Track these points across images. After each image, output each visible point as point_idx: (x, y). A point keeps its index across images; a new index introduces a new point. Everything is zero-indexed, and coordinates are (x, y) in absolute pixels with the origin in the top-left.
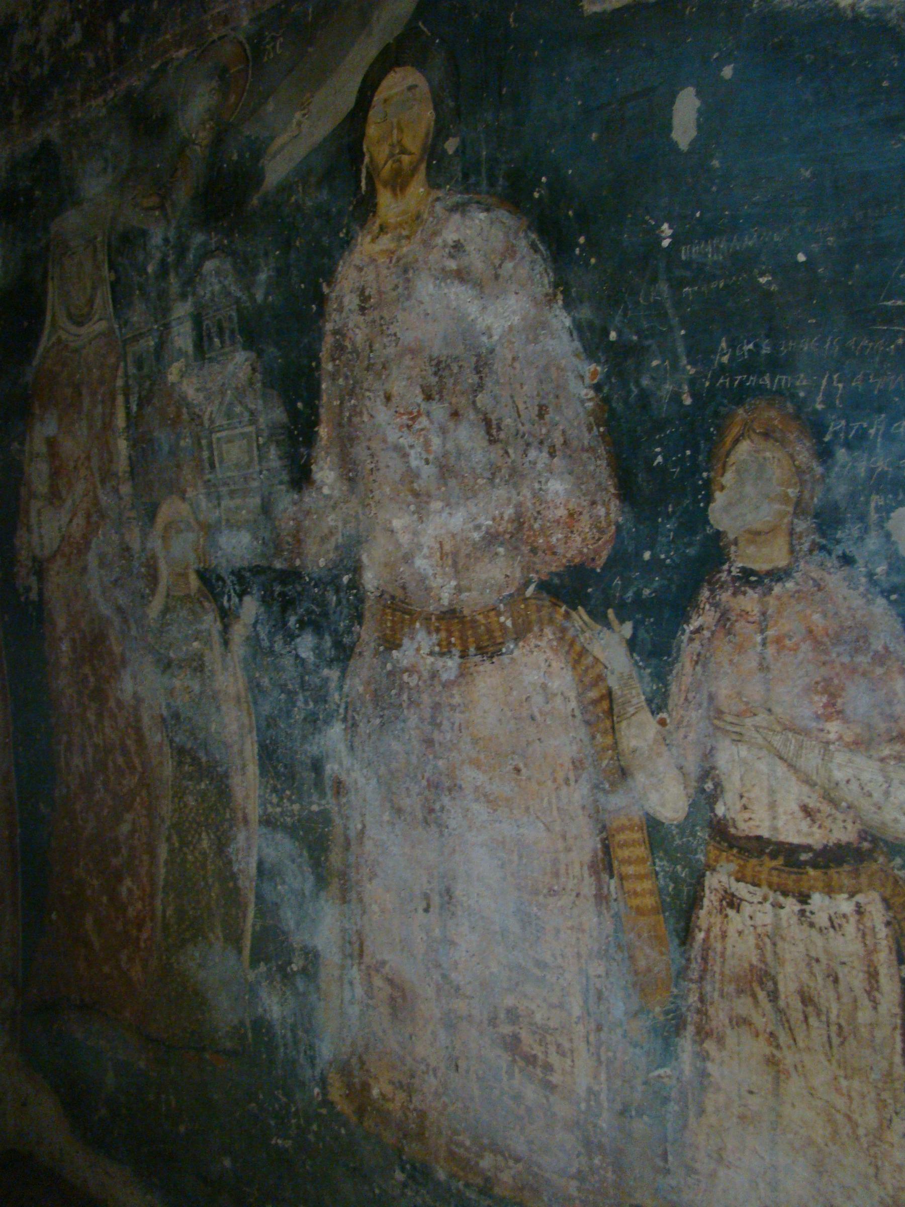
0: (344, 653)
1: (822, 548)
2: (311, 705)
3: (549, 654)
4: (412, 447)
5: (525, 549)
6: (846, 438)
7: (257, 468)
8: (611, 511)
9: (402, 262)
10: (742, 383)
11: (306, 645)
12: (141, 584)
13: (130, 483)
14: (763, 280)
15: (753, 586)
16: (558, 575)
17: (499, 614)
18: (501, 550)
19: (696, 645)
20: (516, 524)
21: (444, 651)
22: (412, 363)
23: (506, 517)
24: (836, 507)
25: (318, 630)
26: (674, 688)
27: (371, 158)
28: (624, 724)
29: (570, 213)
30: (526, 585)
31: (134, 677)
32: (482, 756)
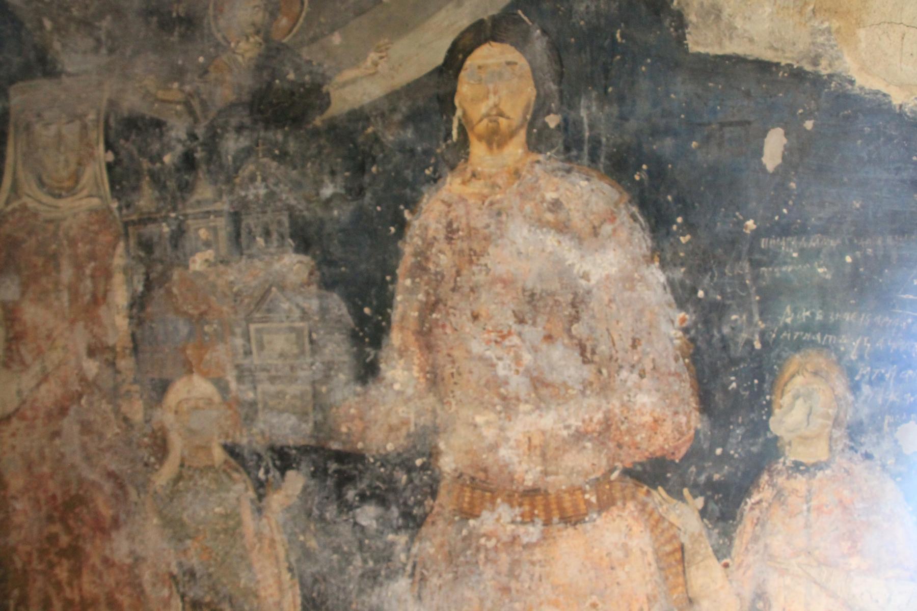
0: (413, 522)
1: (852, 448)
2: (371, 564)
3: (630, 521)
4: (500, 359)
5: (612, 445)
6: (870, 378)
7: (309, 360)
8: (693, 420)
9: (496, 206)
10: (799, 337)
11: (368, 515)
12: (144, 453)
13: (133, 358)
14: (820, 270)
15: (802, 473)
16: (641, 464)
17: (584, 492)
18: (589, 445)
19: (757, 512)
20: (604, 426)
21: (528, 519)
22: (503, 291)
23: (595, 420)
24: (861, 423)
25: (383, 501)
26: (737, 542)
27: (465, 113)
28: (693, 569)
29: (669, 198)
30: (612, 471)
31: (131, 537)
32: (561, 598)
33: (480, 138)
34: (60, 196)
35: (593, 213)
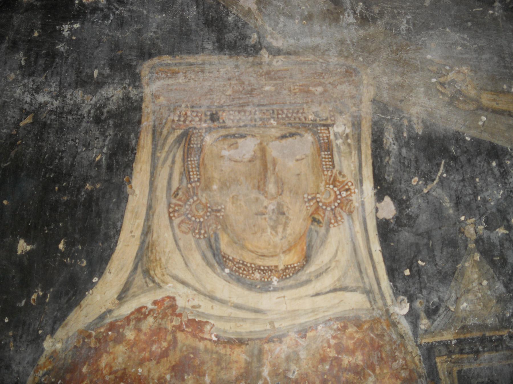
34: (265, 287)
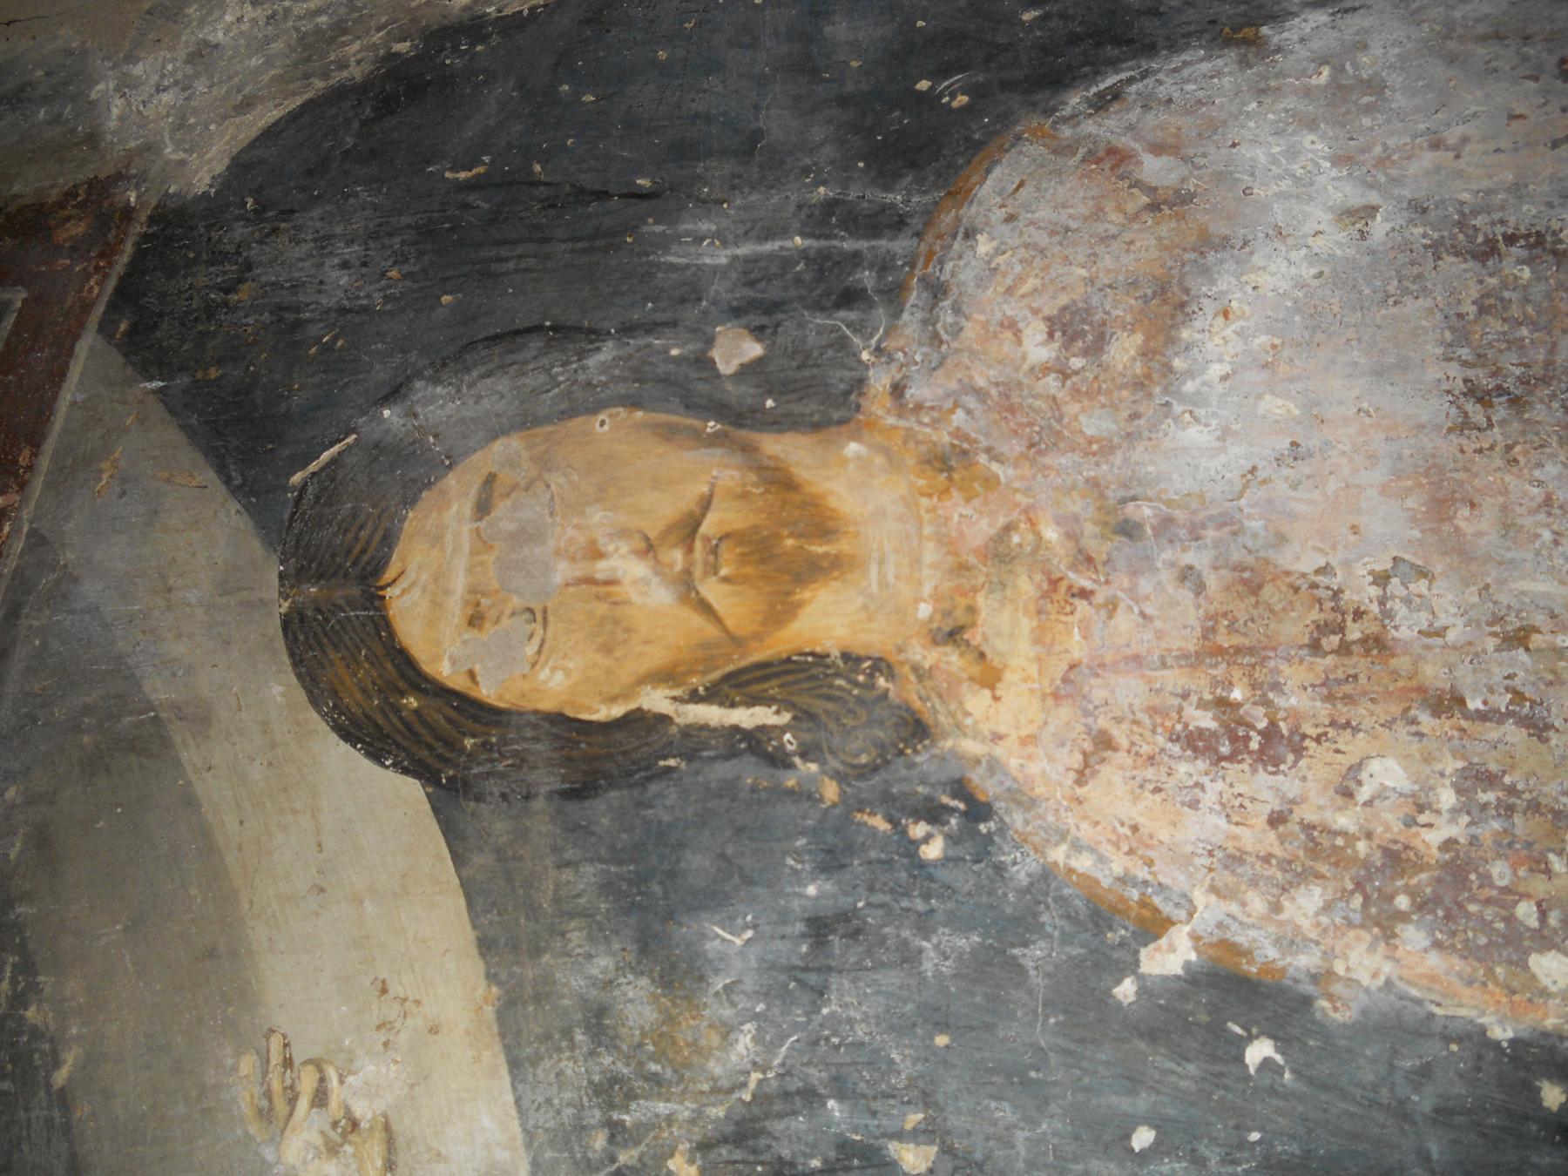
9: (1093, 545)
27: (665, 676)
33: (781, 611)
35: (1098, 214)
